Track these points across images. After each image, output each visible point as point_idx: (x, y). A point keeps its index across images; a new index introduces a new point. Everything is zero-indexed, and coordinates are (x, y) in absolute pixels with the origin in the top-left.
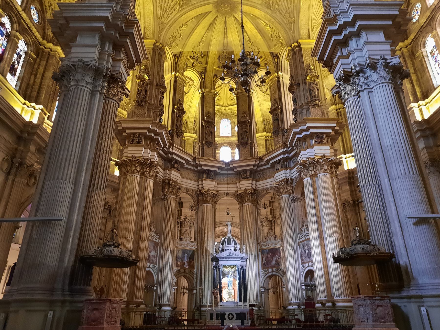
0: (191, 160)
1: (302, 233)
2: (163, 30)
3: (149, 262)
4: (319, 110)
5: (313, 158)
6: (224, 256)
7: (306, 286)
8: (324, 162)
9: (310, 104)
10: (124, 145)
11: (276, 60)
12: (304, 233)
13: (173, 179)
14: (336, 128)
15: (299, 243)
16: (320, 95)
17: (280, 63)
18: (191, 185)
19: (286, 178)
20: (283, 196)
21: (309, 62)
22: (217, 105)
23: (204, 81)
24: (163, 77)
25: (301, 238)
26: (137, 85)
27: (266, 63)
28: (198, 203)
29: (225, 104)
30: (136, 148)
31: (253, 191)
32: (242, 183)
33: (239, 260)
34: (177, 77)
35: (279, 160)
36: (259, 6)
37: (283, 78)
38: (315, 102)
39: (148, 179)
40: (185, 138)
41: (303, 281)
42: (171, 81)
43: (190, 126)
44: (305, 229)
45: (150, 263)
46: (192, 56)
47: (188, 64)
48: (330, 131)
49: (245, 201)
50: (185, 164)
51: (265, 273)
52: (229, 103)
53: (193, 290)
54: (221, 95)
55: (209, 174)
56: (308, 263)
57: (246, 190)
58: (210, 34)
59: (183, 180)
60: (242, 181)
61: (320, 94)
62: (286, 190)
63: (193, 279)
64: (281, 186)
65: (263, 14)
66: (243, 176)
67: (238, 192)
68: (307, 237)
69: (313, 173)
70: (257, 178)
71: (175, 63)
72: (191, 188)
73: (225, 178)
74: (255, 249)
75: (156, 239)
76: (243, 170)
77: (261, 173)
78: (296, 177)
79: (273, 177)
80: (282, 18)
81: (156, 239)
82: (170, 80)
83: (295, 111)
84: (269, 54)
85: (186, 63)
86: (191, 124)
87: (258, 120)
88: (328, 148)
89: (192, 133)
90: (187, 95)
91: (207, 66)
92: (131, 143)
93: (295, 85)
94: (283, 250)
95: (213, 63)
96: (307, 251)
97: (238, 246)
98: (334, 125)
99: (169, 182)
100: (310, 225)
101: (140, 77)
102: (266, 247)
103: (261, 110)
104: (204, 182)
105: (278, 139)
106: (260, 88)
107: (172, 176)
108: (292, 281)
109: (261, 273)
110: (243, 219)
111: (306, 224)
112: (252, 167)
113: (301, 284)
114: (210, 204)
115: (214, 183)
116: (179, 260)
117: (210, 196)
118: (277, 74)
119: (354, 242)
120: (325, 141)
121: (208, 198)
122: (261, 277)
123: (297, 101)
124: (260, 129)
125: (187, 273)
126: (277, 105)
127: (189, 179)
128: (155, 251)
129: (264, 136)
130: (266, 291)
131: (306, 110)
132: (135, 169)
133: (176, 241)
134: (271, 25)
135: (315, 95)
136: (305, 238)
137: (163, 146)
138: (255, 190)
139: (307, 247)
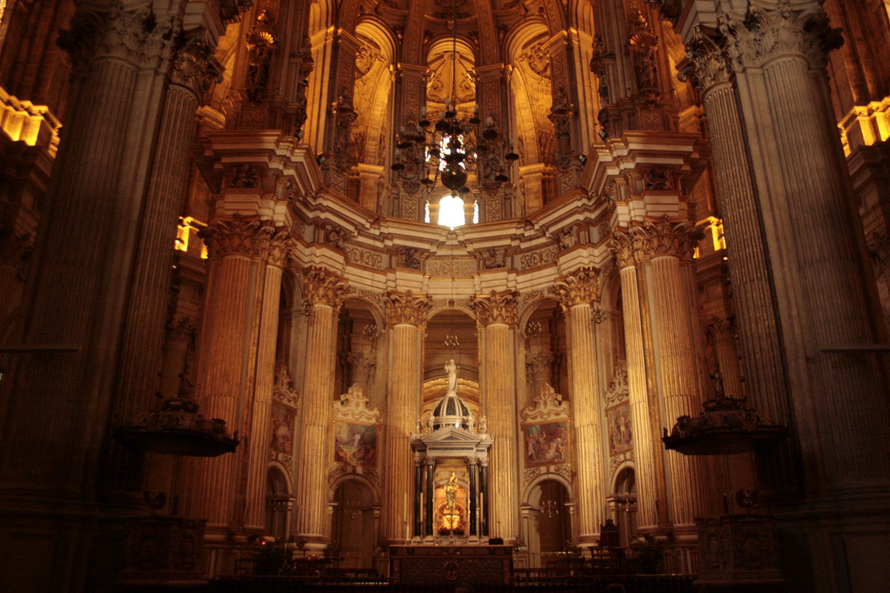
0: (368, 225)
1: (614, 389)
3: (276, 449)
4: (656, 114)
5: (642, 223)
6: (440, 439)
7: (617, 501)
8: (665, 231)
9: (637, 101)
10: (218, 191)
12: (619, 389)
13: (328, 267)
14: (692, 156)
15: (607, 411)
16: (659, 82)
17: (574, 8)
18: (368, 282)
19: (584, 268)
20: (576, 307)
21: (635, 7)
22: (433, 101)
23: (401, 46)
24: (306, 36)
25: (613, 401)
26: (248, 56)
27: (542, 8)
30: (243, 196)
31: (510, 297)
33: (472, 449)
34: (340, 37)
35: (570, 227)
37: (579, 41)
38: (648, 96)
39: (269, 267)
40: (358, 174)
41: (612, 491)
42: (325, 46)
43: (371, 147)
44: (622, 381)
47: (365, 7)
48: (680, 161)
49: (491, 320)
50: (356, 234)
51: (532, 476)
53: (373, 510)
56: (624, 452)
57: (494, 293)
59: (349, 269)
61: (658, 78)
62: (582, 295)
63: (374, 486)
67: (475, 297)
68: (625, 399)
69: (641, 253)
71: (336, 4)
73: (447, 267)
75: (290, 401)
76: (488, 249)
77: (530, 254)
79: (555, 263)
81: (290, 401)
82: (323, 43)
83: (604, 115)
85: (362, 6)
86: (373, 143)
87: (527, 134)
88: (675, 199)
89: (374, 164)
90: (364, 77)
91: (409, 13)
92: (232, 187)
93: (605, 57)
94: (573, 428)
96: (623, 429)
97: (471, 419)
98: (689, 148)
100: (631, 371)
101: (254, 39)
103: (534, 113)
105: (567, 179)
106: (530, 64)
108: (587, 491)
109: (522, 476)
111: (624, 369)
112: (507, 242)
113: (607, 498)
114: (411, 326)
116: (341, 446)
117: (412, 307)
118: (565, 33)
119: (711, 405)
120: (668, 184)
121: (408, 311)
122: (521, 484)
123: (609, 93)
124: (532, 156)
125: (359, 475)
126: (565, 102)
128: (289, 426)
129: (540, 171)
130: (532, 512)
131: (629, 115)
132: (240, 245)
133: (335, 406)
135: (649, 81)
136: (620, 400)
137: (303, 193)
138: (515, 294)
139: (623, 419)
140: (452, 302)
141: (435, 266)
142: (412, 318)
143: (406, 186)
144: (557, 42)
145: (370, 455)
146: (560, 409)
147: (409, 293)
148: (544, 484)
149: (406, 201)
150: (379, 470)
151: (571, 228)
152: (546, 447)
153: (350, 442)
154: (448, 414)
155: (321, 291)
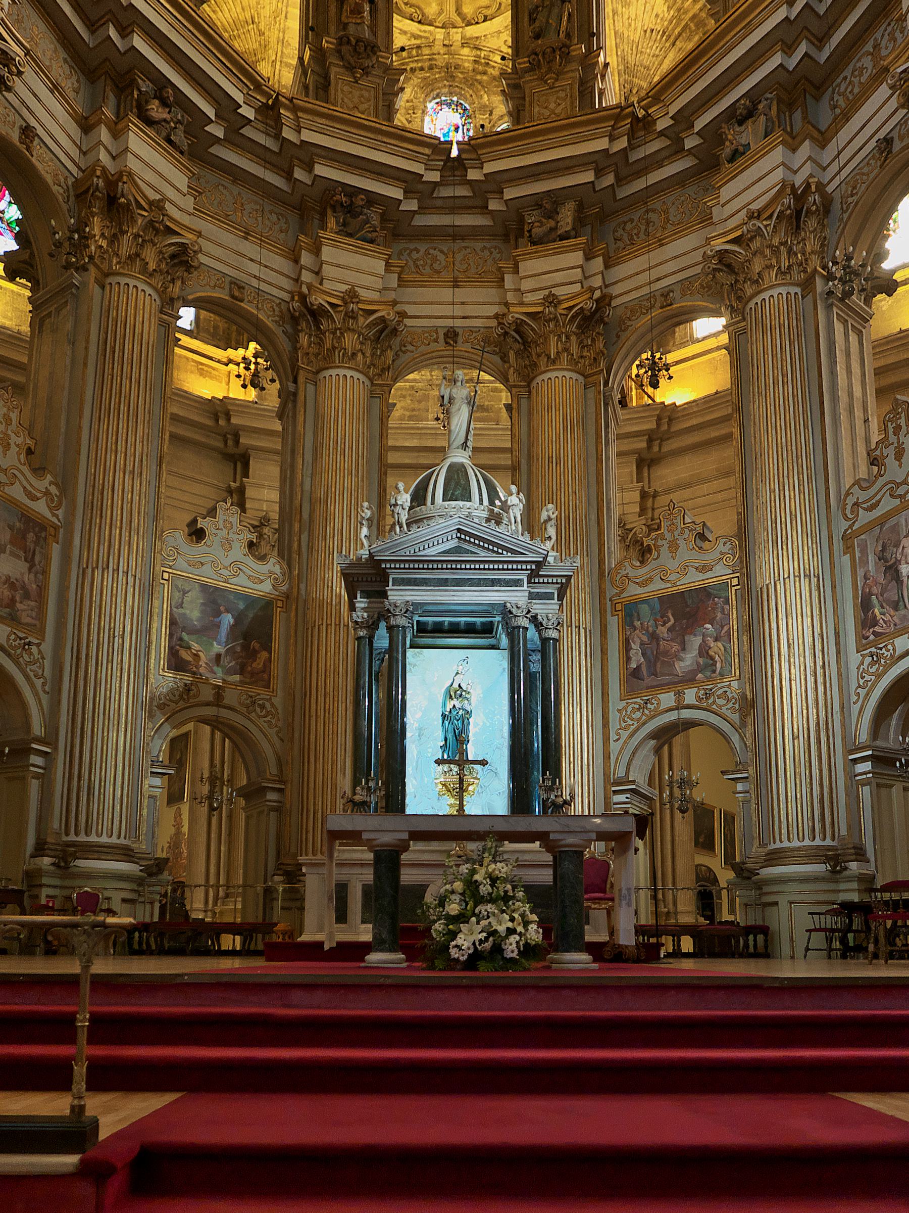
20: (766, 295)
28: (292, 372)
31: (590, 305)
49: (543, 361)
55: (355, 216)
57: (552, 300)
60: (529, 256)
62: (785, 264)
64: (756, 244)
66: (537, 231)
72: (255, 283)
73: (441, 257)
74: (592, 598)
76: (537, 202)
78: (853, 182)
79: (706, 219)
104: (327, 253)
110: (530, 457)
112: (588, 176)
114: (357, 375)
115: (380, 266)
121: (350, 341)
127: (246, 235)
141: (415, 255)
142: (360, 354)
143: (345, 49)
147: (351, 295)
149: (346, 88)
151: (755, 105)
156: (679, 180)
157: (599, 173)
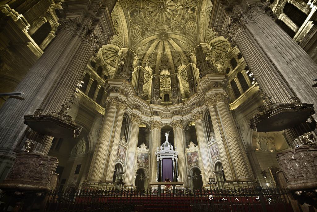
2: (133, 45)
3: (120, 158)
6: (164, 153)
7: (216, 173)
11: (189, 58)
12: (212, 140)
15: (209, 147)
29: (166, 87)
31: (181, 121)
32: (175, 117)
36: (179, 34)
41: (214, 170)
45: (121, 159)
46: (149, 60)
52: (168, 86)
54: (164, 83)
57: (177, 120)
58: (157, 50)
65: (181, 37)
68: (214, 142)
70: (183, 114)
76: (175, 111)
79: (191, 112)
80: (191, 37)
84: (185, 56)
95: (159, 64)
96: (215, 151)
99: (134, 116)
102: (190, 151)
107: (136, 112)
128: (124, 152)
130: (191, 178)
134: (186, 42)
138: (182, 121)
139: (214, 148)
140: (167, 124)
144: (188, 66)
145: (147, 162)
146: (196, 147)
148: (193, 169)
150: (149, 166)
152: (193, 158)
153: (141, 158)
154: (166, 146)
155: (135, 119)
156: (189, 109)
157: (181, 108)
